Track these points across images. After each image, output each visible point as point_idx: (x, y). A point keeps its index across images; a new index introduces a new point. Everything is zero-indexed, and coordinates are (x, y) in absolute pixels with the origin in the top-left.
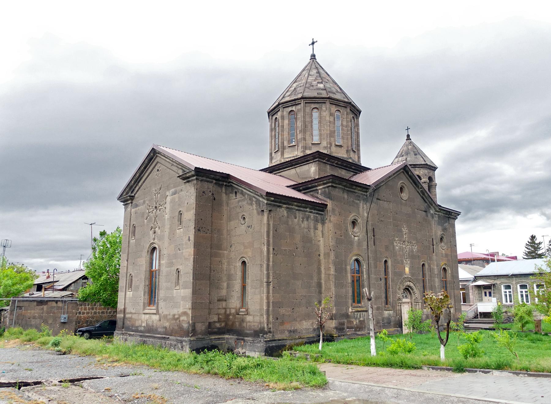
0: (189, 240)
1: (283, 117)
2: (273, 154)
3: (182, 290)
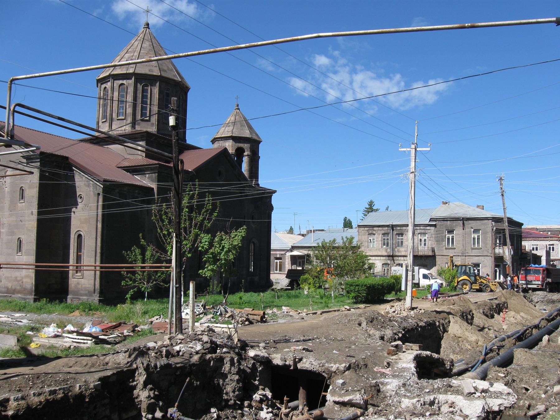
0: (32, 213)
1: (113, 88)
2: (100, 123)
3: (25, 257)
